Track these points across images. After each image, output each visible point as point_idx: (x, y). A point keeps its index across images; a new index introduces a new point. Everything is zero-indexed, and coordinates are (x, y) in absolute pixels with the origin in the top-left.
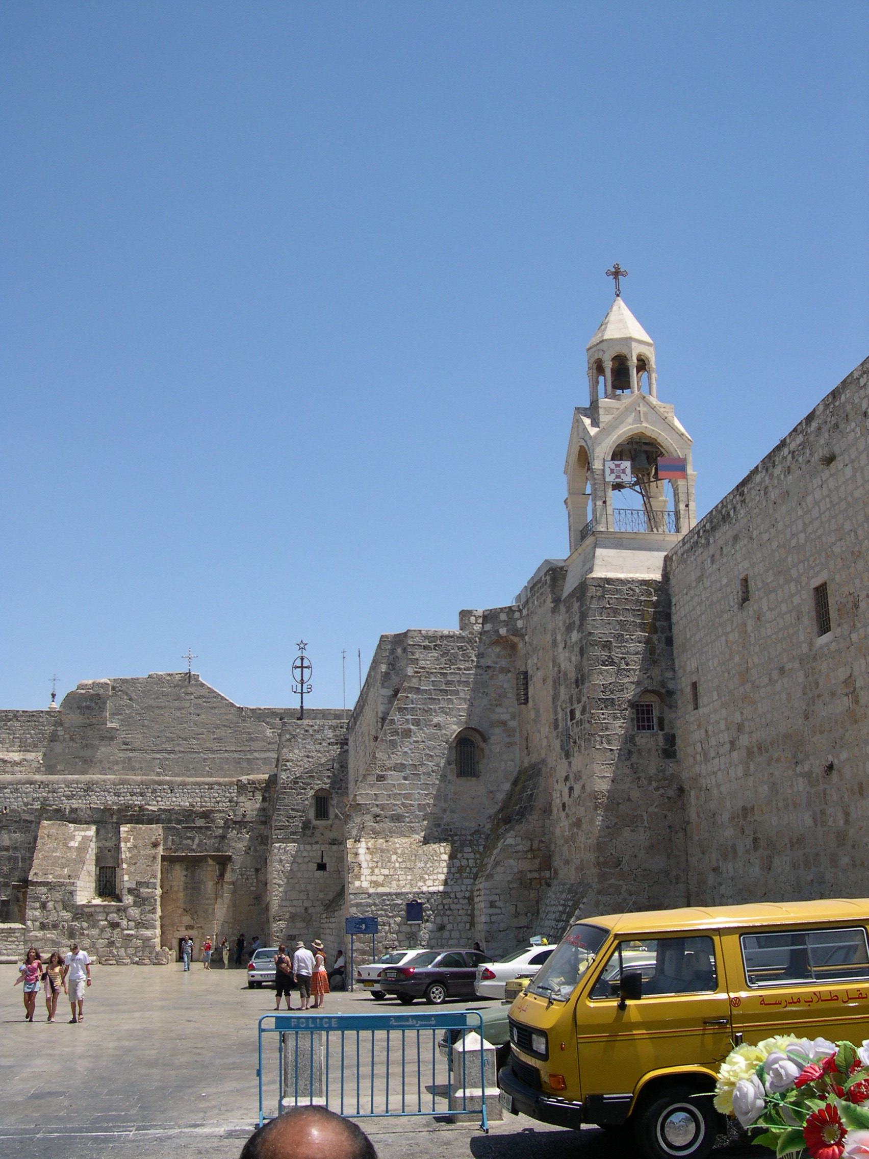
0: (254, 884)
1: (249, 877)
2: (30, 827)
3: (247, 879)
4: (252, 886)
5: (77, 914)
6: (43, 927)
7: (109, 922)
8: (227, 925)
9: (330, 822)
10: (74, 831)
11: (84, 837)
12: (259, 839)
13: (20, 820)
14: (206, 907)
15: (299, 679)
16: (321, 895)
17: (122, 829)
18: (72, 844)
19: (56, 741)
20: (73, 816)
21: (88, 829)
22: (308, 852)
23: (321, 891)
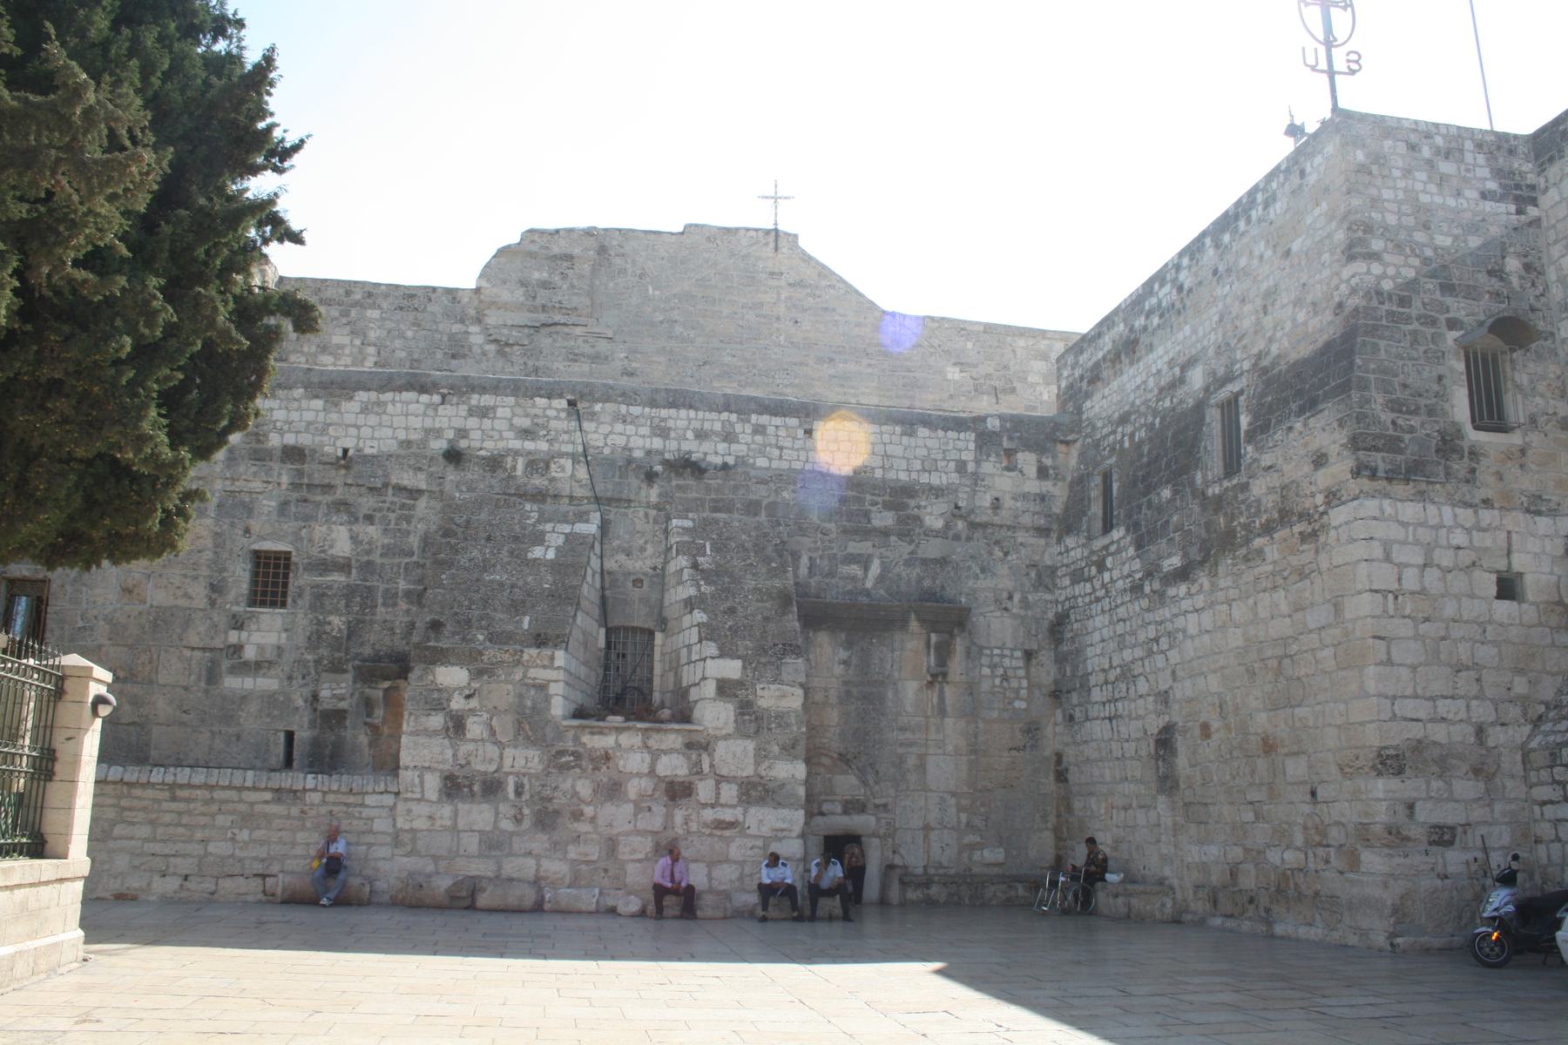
0: (1023, 693)
1: (1010, 673)
2: (412, 508)
3: (1005, 678)
4: (1018, 698)
5: (561, 753)
6: (453, 787)
7: (661, 779)
8: (953, 801)
9: (1516, 439)
10: (539, 521)
11: (569, 537)
12: (1033, 574)
13: (386, 485)
14: (900, 750)
15: (1321, 37)
16: (1520, 686)
17: (674, 521)
18: (537, 552)
19: (464, 356)
20: (538, 481)
21: (582, 517)
22: (1468, 531)
23: (1520, 672)
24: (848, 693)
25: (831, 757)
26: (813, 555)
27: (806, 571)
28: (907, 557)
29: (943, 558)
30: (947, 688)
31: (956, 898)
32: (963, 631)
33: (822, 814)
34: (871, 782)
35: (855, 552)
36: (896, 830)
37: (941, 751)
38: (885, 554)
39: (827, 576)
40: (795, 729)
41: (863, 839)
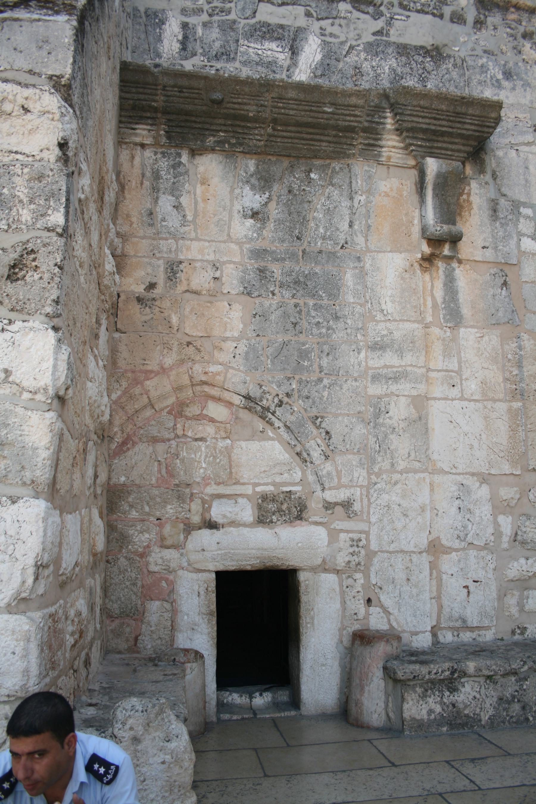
8: (484, 492)
14: (375, 390)
24: (262, 271)
25: (229, 404)
26: (192, 20)
27: (176, 46)
28: (372, 39)
29: (437, 48)
30: (459, 272)
31: (516, 707)
32: (482, 171)
33: (212, 525)
34: (316, 454)
35: (274, 20)
36: (371, 555)
37: (455, 392)
38: (329, 30)
39: (217, 57)
40: (26, 215)
41: (302, 577)
